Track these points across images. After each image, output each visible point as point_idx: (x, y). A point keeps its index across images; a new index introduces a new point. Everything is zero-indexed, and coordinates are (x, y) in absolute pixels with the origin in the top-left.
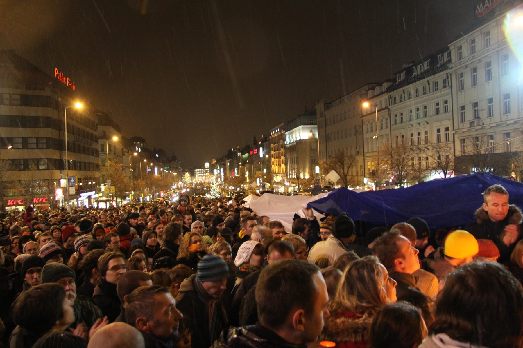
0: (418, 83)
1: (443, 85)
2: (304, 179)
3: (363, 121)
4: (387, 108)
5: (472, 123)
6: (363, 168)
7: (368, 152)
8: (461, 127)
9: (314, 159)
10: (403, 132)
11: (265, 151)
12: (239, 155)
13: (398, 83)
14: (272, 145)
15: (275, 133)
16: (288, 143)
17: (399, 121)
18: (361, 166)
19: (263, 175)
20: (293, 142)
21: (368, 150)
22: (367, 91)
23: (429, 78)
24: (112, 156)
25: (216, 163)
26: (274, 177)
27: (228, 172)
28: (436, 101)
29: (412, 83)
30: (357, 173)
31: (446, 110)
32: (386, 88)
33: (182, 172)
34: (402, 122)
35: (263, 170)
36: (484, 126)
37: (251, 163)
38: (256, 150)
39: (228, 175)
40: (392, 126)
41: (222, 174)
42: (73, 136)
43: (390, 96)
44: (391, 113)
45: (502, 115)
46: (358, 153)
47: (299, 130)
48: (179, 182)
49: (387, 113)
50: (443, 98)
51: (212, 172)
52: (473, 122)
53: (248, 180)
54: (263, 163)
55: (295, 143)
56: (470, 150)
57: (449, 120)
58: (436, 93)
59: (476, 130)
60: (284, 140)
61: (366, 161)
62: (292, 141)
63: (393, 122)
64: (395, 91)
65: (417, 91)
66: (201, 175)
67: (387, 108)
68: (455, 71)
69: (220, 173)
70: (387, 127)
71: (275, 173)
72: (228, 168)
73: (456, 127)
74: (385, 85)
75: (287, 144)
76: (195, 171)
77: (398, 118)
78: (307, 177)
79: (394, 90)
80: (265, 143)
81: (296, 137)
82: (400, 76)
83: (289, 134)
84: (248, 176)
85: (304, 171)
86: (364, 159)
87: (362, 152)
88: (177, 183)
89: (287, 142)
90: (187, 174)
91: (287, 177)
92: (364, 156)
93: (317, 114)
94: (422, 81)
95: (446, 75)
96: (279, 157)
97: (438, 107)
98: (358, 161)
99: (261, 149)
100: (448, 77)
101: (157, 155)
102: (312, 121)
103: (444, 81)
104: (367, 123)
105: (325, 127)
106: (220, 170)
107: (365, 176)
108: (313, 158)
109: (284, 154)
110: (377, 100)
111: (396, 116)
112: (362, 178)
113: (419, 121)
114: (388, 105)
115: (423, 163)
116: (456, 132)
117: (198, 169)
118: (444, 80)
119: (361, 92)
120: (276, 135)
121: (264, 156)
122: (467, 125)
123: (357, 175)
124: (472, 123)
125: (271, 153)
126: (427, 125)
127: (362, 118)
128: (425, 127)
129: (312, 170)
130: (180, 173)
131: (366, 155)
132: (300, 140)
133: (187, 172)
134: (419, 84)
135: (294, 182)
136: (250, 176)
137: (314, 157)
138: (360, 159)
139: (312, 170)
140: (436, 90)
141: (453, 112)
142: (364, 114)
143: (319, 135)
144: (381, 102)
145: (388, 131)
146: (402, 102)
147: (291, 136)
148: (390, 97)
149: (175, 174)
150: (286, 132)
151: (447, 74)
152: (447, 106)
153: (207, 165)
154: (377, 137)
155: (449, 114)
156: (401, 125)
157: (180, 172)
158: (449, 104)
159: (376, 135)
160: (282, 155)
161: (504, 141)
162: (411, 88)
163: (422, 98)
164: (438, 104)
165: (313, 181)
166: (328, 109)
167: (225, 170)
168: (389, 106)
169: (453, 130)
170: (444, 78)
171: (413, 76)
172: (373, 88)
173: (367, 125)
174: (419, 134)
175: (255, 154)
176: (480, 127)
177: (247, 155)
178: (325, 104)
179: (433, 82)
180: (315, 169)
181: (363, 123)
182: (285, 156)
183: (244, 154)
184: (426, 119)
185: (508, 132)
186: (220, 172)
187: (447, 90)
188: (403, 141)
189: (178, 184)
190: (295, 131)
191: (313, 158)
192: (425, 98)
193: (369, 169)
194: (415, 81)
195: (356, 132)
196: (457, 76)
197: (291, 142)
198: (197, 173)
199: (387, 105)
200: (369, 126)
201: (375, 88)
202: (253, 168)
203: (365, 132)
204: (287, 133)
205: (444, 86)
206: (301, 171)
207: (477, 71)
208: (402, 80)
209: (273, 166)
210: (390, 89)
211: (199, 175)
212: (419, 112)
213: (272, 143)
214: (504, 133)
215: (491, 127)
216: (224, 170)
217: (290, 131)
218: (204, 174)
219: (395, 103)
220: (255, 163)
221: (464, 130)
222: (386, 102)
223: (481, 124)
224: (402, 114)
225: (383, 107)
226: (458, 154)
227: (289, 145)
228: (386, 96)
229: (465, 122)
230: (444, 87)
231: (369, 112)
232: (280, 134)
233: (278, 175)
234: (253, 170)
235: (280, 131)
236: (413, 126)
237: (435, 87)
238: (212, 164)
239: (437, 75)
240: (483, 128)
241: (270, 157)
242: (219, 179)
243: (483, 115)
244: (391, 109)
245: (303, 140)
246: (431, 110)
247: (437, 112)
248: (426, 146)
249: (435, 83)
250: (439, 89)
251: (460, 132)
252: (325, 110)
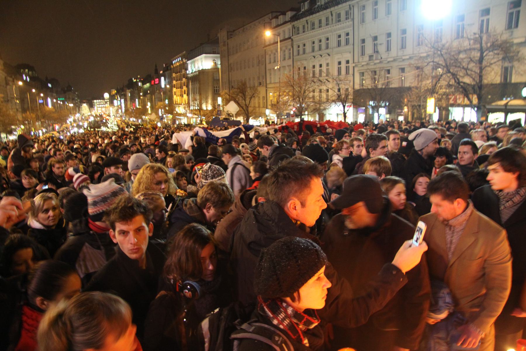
0: (321, 13)
1: (345, 17)
2: (207, 110)
3: (266, 51)
4: (290, 38)
5: (371, 57)
6: (265, 99)
7: (271, 83)
8: (361, 60)
9: (217, 90)
10: (305, 63)
11: (167, 81)
12: (140, 85)
13: (301, 12)
14: (174, 75)
15: (176, 62)
16: (190, 73)
17: (301, 52)
18: (263, 97)
19: (165, 106)
20: (195, 72)
21: (271, 81)
22: (271, 20)
23: (332, 9)
25: (116, 94)
26: (175, 108)
27: (129, 103)
28: (338, 32)
29: (316, 13)
30: (259, 103)
31: (347, 43)
32: (290, 17)
33: (79, 103)
34: (304, 53)
35: (165, 100)
36: (382, 60)
37: (153, 93)
38: (158, 79)
39: (129, 106)
40: (294, 58)
41: (123, 105)
43: (294, 25)
44: (294, 44)
45: (399, 50)
46: (260, 84)
47: (201, 59)
48: (76, 114)
49: (290, 43)
50: (345, 30)
51: (112, 103)
52: (372, 56)
53: (149, 112)
54: (165, 93)
55: (197, 73)
56: (368, 83)
57: (350, 52)
58: (338, 25)
59: (375, 64)
60: (186, 69)
61: (268, 92)
62: (194, 70)
63: (295, 53)
64: (298, 21)
65: (320, 22)
66: (100, 106)
67: (290, 38)
68: (358, 2)
69: (121, 105)
70: (290, 58)
71: (178, 104)
72: (128, 99)
73: (356, 60)
74: (289, 14)
75: (189, 74)
76: (94, 102)
77: (301, 49)
78: (210, 108)
79: (297, 19)
80: (167, 73)
81: (198, 67)
82: (304, 5)
83: (191, 63)
84: (150, 107)
85: (207, 102)
86: (266, 90)
87: (265, 82)
88: (73, 115)
89: (189, 72)
90: (85, 106)
91: (190, 108)
92: (266, 87)
93: (220, 42)
94: (325, 11)
95: (348, 7)
96: (181, 88)
97: (339, 39)
98: (260, 92)
99: (163, 79)
100: (350, 8)
102: (214, 50)
103: (347, 13)
105: (228, 56)
106: (120, 101)
107: (267, 108)
108: (216, 89)
109: (186, 84)
110: (280, 30)
111: (299, 47)
112: (263, 109)
113: (320, 52)
114: (291, 35)
115: (324, 95)
116: (356, 66)
117: (96, 99)
118: (346, 12)
119: (264, 21)
120: (178, 64)
121: (165, 85)
122: (366, 58)
123: (259, 107)
124: (371, 57)
125: (173, 83)
126: (328, 57)
127: (265, 48)
128: (327, 59)
129: (214, 100)
130: (77, 105)
131: (269, 86)
132: (202, 70)
133: (84, 103)
134: (322, 15)
135: (196, 113)
136: (152, 107)
137: (217, 87)
138: (262, 90)
139: (214, 100)
140: (338, 22)
141: (353, 45)
142: (267, 43)
143: (221, 64)
144: (284, 32)
145: (290, 62)
146: (305, 33)
147: (193, 65)
148: (294, 27)
149: (71, 105)
150: (188, 61)
151: (350, 5)
152: (349, 38)
153: (106, 95)
155: (350, 47)
156: (304, 56)
157: (77, 103)
158: (351, 37)
160: (184, 85)
161: (399, 76)
162: (314, 18)
163: (324, 29)
164: (339, 36)
165: (215, 112)
166: (231, 37)
167: (126, 101)
168: (293, 36)
169: (354, 63)
170: (347, 10)
171: (317, 6)
173: (270, 55)
174: (321, 66)
175: (157, 84)
176: (378, 61)
177: (148, 85)
178: (228, 32)
179: (336, 13)
180: (217, 100)
182: (187, 86)
183: (146, 84)
184: (328, 51)
185: (403, 67)
186: (121, 103)
187: (349, 22)
188: (305, 73)
189: (75, 116)
190: (198, 60)
191: (216, 89)
192: (327, 29)
193: (271, 101)
194: (319, 12)
195: (259, 63)
196: (360, 9)
197: (193, 72)
198: (96, 104)
199: (290, 35)
200: (272, 56)
201: (279, 17)
202: (155, 98)
203: (267, 61)
204: (189, 62)
205: (346, 18)
206: (203, 102)
207: (378, 4)
208: (306, 9)
209: (175, 97)
210: (294, 18)
211: (98, 106)
212: (322, 43)
213: (174, 73)
214: (400, 69)
215: (389, 62)
216: (124, 101)
217: (192, 60)
218: (104, 106)
219: (298, 34)
220: (156, 94)
221: (363, 64)
222: (290, 32)
223: (380, 58)
224: (304, 45)
225: (287, 37)
226: (357, 87)
227: (192, 75)
228: (289, 26)
229: (364, 55)
230: (346, 19)
231: (272, 42)
232: (182, 62)
233: (180, 106)
234: (155, 100)
235: (182, 60)
236: (314, 57)
237: (338, 18)
238: (112, 94)
239: (340, 6)
240: (381, 62)
241: (172, 86)
242: (120, 111)
243: (382, 49)
244: (294, 39)
245: (205, 69)
246: (333, 42)
247: (339, 44)
248: (327, 78)
249: (338, 14)
250: (341, 20)
251: (359, 66)
252: (228, 39)
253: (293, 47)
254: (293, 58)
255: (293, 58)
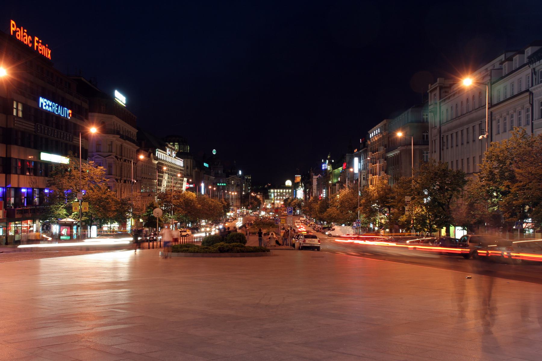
3: (493, 114)
4: (527, 91)
24: (112, 160)
40: (535, 122)
42: (34, 124)
43: (534, 69)
44: (534, 99)
101: (206, 165)
104: (498, 117)
114: (530, 86)
144: (520, 81)
148: (534, 72)
154: (485, 136)
159: (484, 134)
168: (532, 86)
172: (510, 59)
181: (493, 118)
200: (501, 124)
225: (523, 89)
228: (527, 71)
253: (532, 105)
254: (532, 123)
255: (532, 123)
